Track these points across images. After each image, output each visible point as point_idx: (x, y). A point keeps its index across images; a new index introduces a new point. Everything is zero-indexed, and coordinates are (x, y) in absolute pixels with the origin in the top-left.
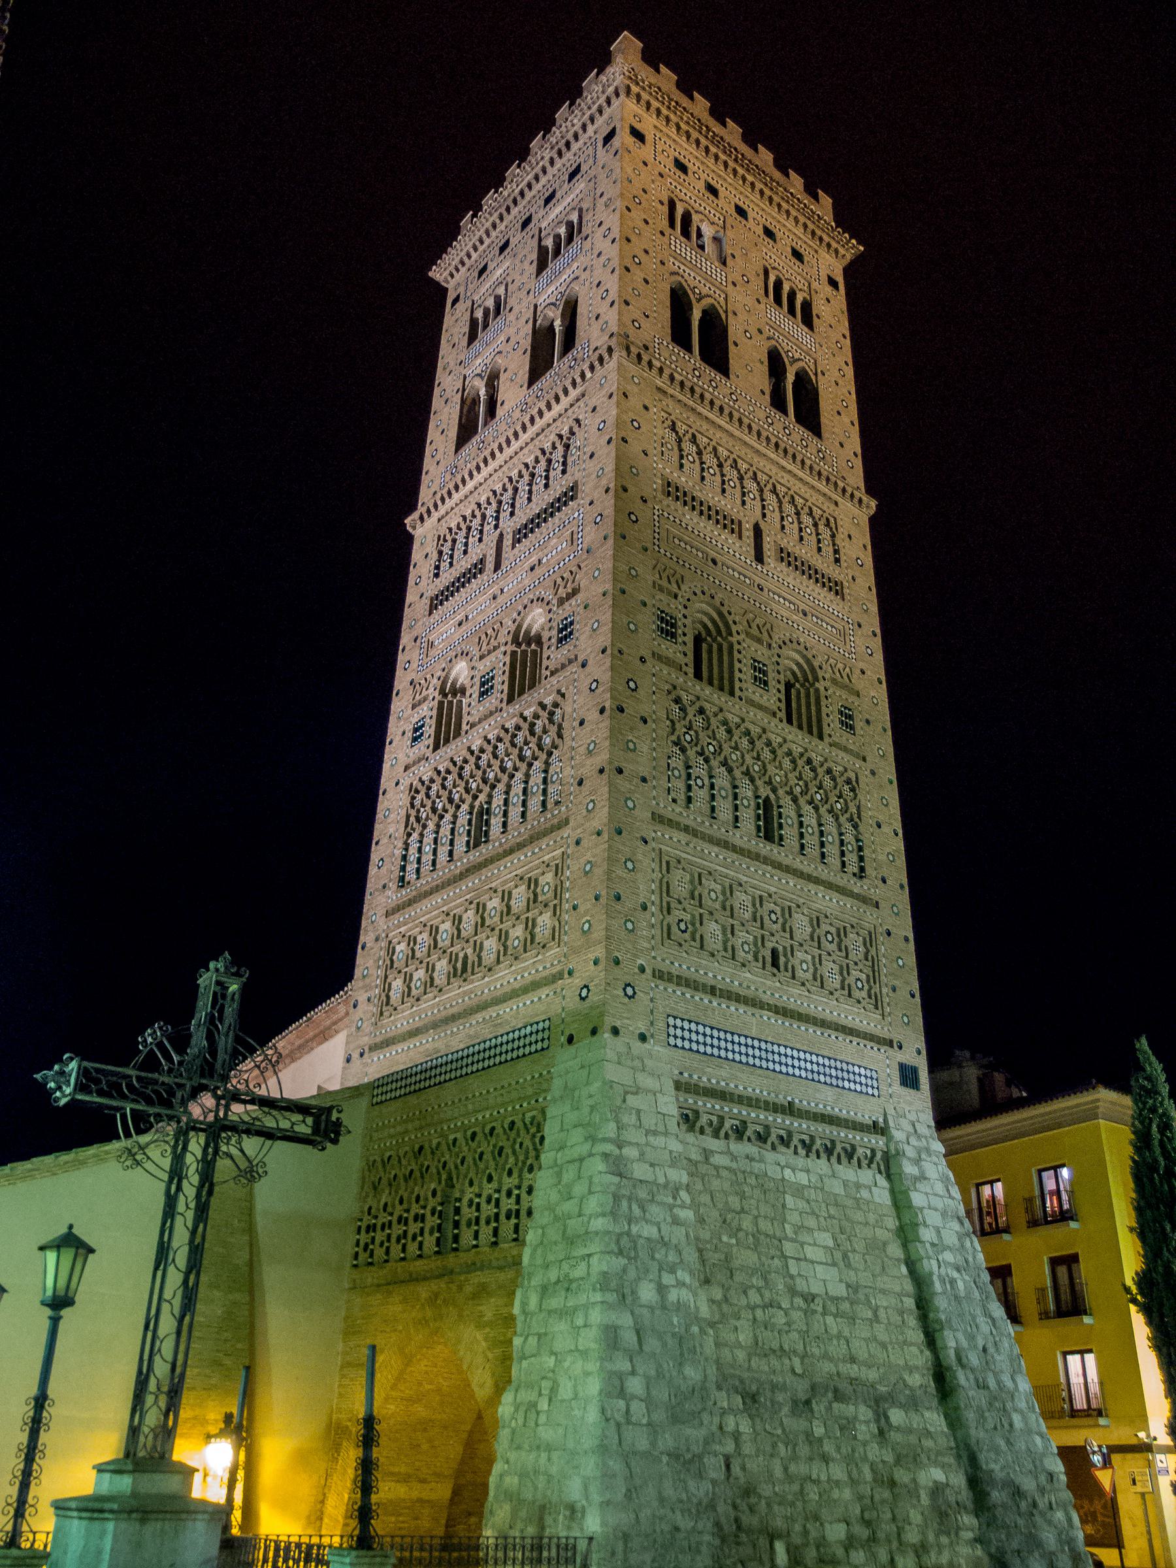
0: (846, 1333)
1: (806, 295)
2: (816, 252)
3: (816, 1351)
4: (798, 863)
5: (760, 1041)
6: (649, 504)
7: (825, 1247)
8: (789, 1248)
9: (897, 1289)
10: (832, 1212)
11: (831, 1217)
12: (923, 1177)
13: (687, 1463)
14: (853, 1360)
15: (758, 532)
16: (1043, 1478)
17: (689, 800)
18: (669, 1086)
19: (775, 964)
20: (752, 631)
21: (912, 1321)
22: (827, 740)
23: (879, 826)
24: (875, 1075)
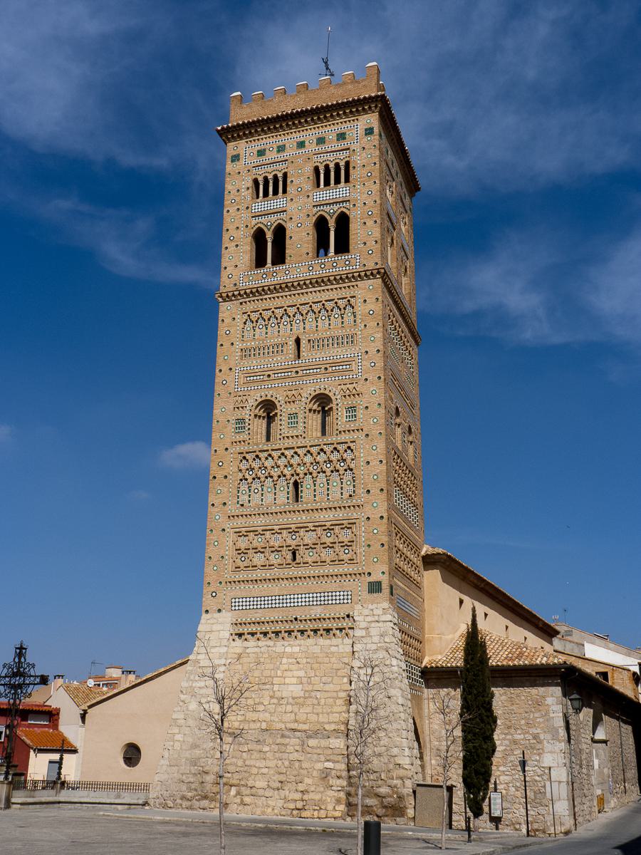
0: (296, 710)
1: (348, 159)
2: (357, 119)
3: (277, 720)
4: (309, 506)
5: (279, 596)
6: (233, 369)
7: (298, 677)
8: (276, 680)
9: (338, 688)
10: (308, 660)
11: (307, 663)
12: (368, 635)
13: (194, 762)
14: (296, 721)
15: (298, 341)
16: (391, 766)
17: (249, 501)
18: (228, 627)
19: (294, 559)
20: (289, 400)
21: (339, 702)
22: (335, 434)
23: (368, 463)
24: (350, 593)
